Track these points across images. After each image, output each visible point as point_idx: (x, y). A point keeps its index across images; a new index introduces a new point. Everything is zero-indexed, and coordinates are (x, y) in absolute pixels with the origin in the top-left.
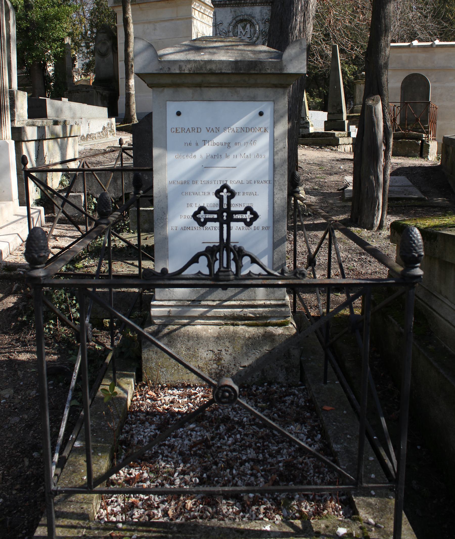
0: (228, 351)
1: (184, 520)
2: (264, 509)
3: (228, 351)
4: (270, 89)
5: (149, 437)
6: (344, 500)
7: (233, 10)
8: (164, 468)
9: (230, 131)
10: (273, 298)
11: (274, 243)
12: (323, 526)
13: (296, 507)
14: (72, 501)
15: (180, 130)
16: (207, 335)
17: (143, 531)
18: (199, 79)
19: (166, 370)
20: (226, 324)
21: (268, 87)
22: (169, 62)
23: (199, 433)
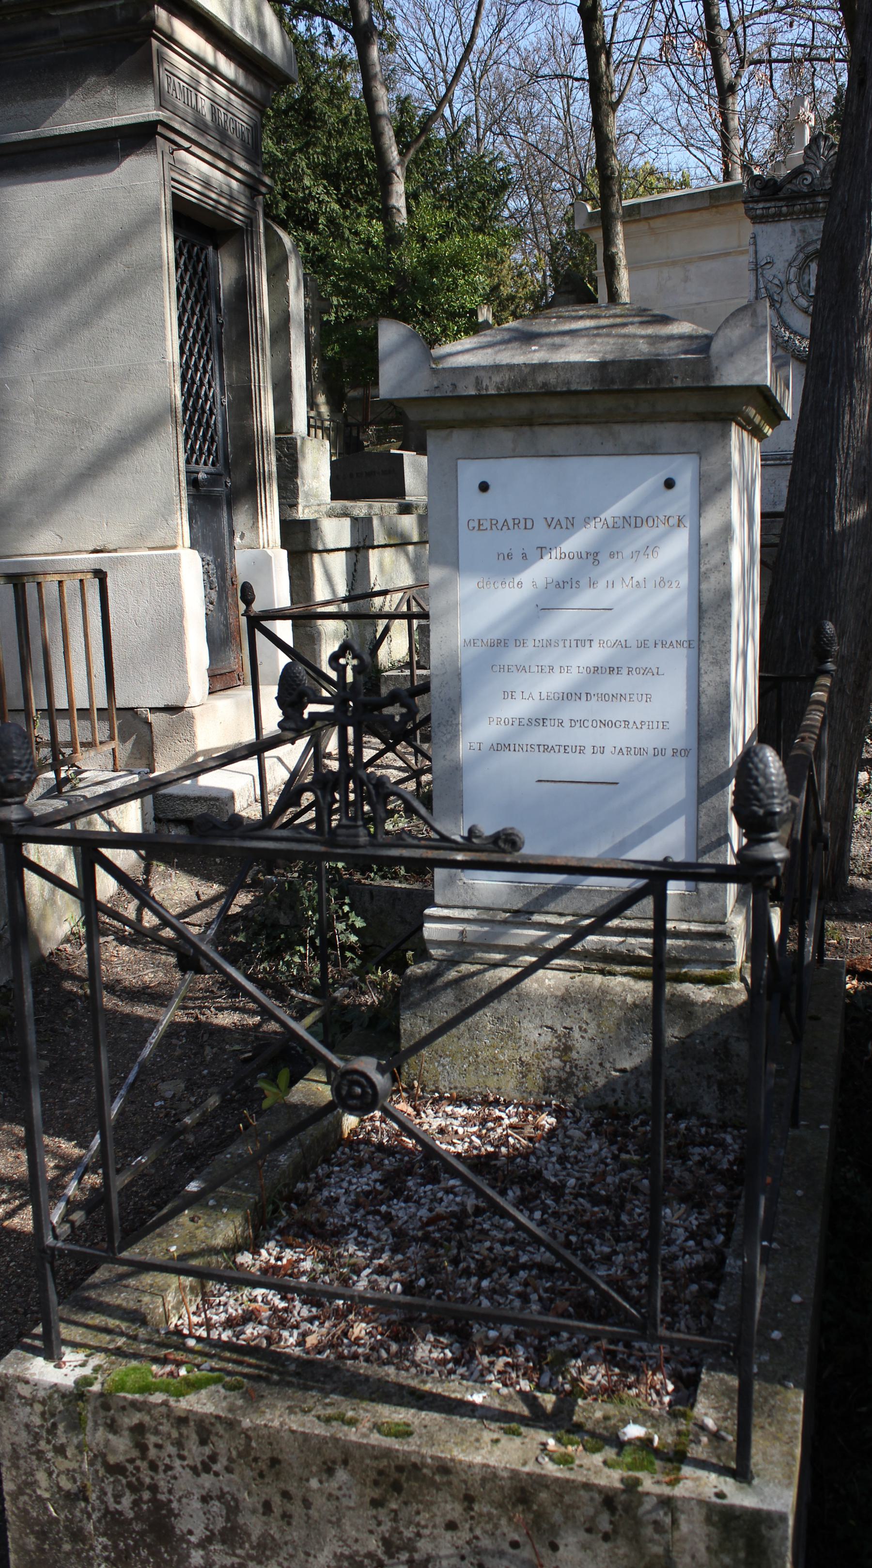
0: (585, 1031)
1: (332, 1357)
2: (507, 1364)
3: (585, 1031)
4: (689, 425)
5: (357, 1194)
6: (688, 1374)
7: (797, 228)
8: (351, 1256)
9: (599, 525)
10: (696, 918)
11: (699, 789)
12: (599, 1414)
13: (574, 1372)
14: (126, 1286)
15: (487, 525)
16: (541, 991)
17: (229, 1360)
18: (523, 408)
19: (451, 1062)
20: (588, 970)
21: (684, 421)
22: (454, 370)
23: (458, 1199)
